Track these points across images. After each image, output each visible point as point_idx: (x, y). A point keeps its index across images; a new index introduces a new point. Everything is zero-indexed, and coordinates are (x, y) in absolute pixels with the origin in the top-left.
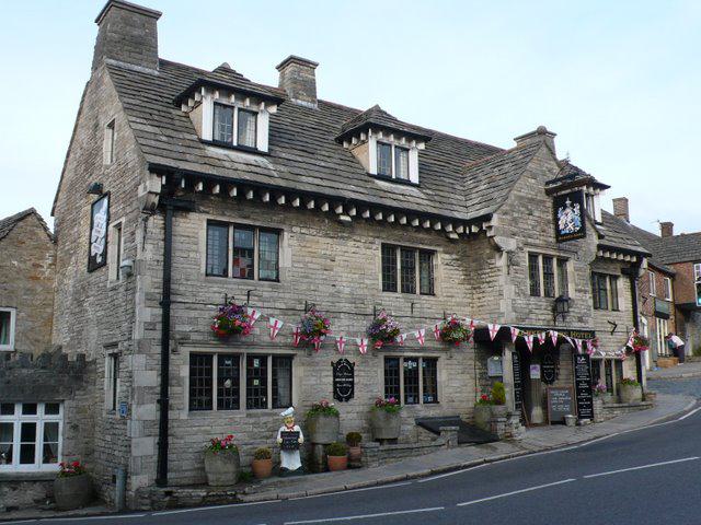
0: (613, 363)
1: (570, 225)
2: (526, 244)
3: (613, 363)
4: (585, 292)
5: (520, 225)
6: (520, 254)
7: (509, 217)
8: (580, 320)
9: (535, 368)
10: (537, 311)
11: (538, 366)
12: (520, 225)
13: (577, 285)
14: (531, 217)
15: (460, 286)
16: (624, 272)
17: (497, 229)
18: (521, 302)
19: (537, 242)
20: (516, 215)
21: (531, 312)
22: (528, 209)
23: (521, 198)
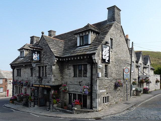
1: (36, 59)
8: (48, 82)
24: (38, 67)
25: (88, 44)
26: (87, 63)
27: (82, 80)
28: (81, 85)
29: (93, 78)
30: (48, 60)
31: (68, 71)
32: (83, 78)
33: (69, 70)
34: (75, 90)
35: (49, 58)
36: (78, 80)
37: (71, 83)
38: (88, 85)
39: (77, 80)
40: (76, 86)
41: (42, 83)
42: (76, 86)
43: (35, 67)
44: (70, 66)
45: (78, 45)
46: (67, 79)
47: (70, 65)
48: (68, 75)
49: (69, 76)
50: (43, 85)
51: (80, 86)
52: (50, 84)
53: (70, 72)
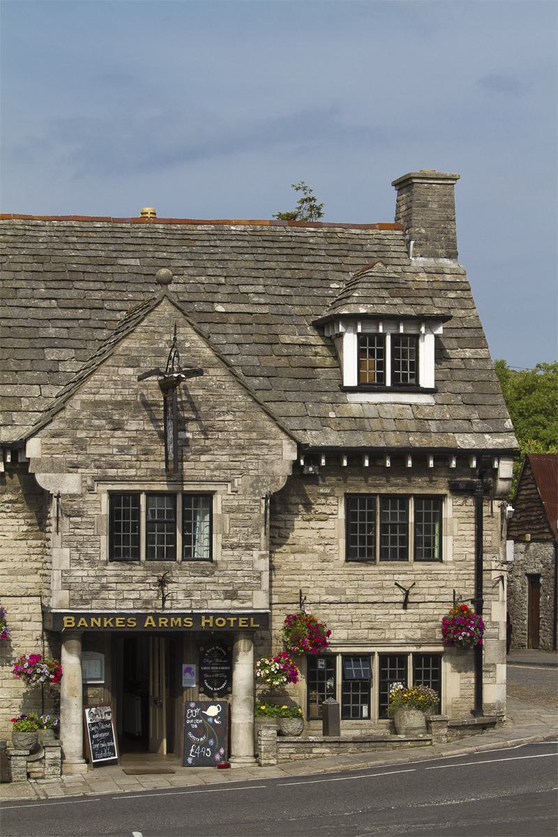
0: (410, 658)
2: (103, 479)
3: (410, 658)
4: (249, 547)
5: (91, 450)
6: (89, 497)
7: (65, 440)
8: (231, 595)
9: (189, 670)
10: (119, 586)
11: (194, 667)
12: (91, 450)
13: (226, 537)
14: (118, 433)
15: (14, 543)
16: (456, 490)
17: (39, 461)
18: (83, 573)
19: (132, 472)
20: (81, 434)
21: (104, 587)
22: (111, 421)
23: (97, 404)
24: (112, 495)
25: (418, 390)
26: (444, 491)
27: (412, 577)
28: (405, 604)
29: (485, 565)
30: (225, 458)
31: (306, 524)
32: (419, 566)
33: (312, 524)
34: (364, 633)
35: (241, 447)
36: (387, 577)
37: (332, 598)
38: (300, 603)
39: (381, 576)
40: (372, 612)
41: (168, 604)
42: (372, 612)
43: (73, 496)
44: (323, 501)
45: (350, 379)
46: (298, 571)
47: (326, 496)
48: (314, 552)
49: (316, 556)
50: (183, 616)
51: (402, 611)
52: (248, 604)
53: (323, 533)
